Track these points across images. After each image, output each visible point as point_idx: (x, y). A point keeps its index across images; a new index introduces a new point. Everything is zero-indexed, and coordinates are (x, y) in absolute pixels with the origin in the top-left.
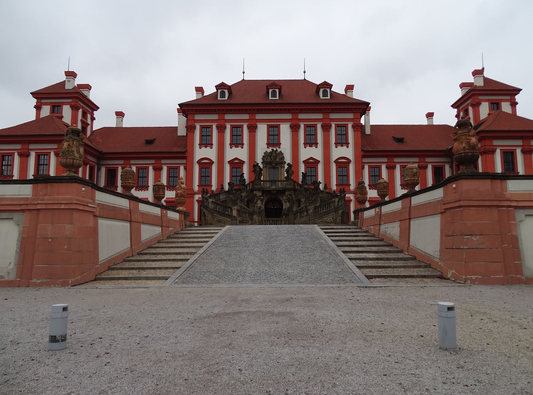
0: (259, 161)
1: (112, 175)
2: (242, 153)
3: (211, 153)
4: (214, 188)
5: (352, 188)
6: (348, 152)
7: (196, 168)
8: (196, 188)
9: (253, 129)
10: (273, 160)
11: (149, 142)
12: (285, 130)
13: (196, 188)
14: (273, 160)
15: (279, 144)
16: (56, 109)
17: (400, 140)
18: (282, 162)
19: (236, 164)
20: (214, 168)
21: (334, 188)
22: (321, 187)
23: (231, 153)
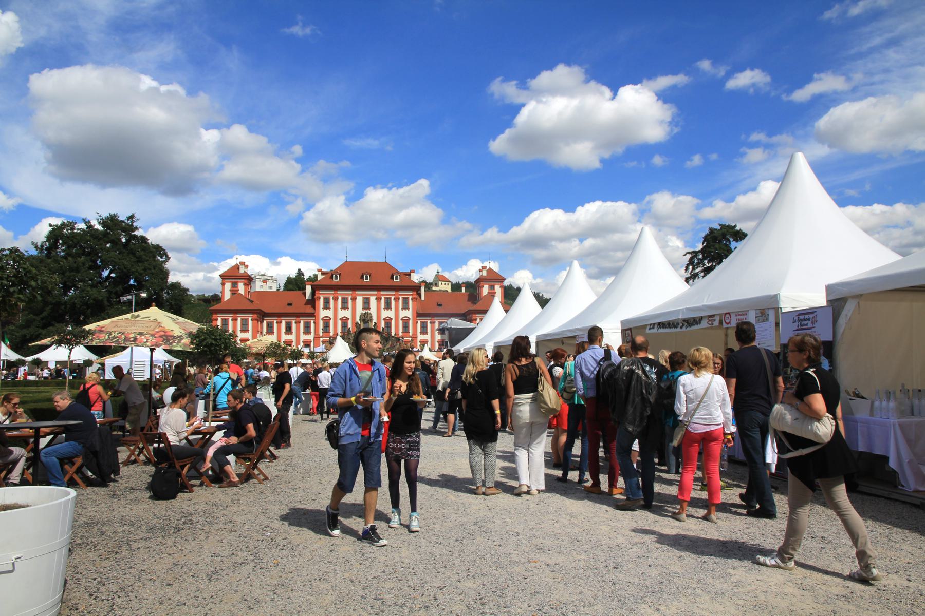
0: (358, 320)
1: (270, 326)
2: (347, 314)
3: (329, 313)
4: (332, 334)
5: (411, 334)
6: (409, 313)
7: (321, 323)
8: (321, 334)
9: (354, 299)
10: (366, 318)
11: (290, 304)
12: (373, 300)
13: (321, 334)
14: (366, 318)
15: (369, 309)
16: (234, 285)
17: (440, 305)
18: (371, 320)
19: (345, 321)
20: (332, 322)
21: (401, 334)
22: (393, 334)
23: (342, 314)
